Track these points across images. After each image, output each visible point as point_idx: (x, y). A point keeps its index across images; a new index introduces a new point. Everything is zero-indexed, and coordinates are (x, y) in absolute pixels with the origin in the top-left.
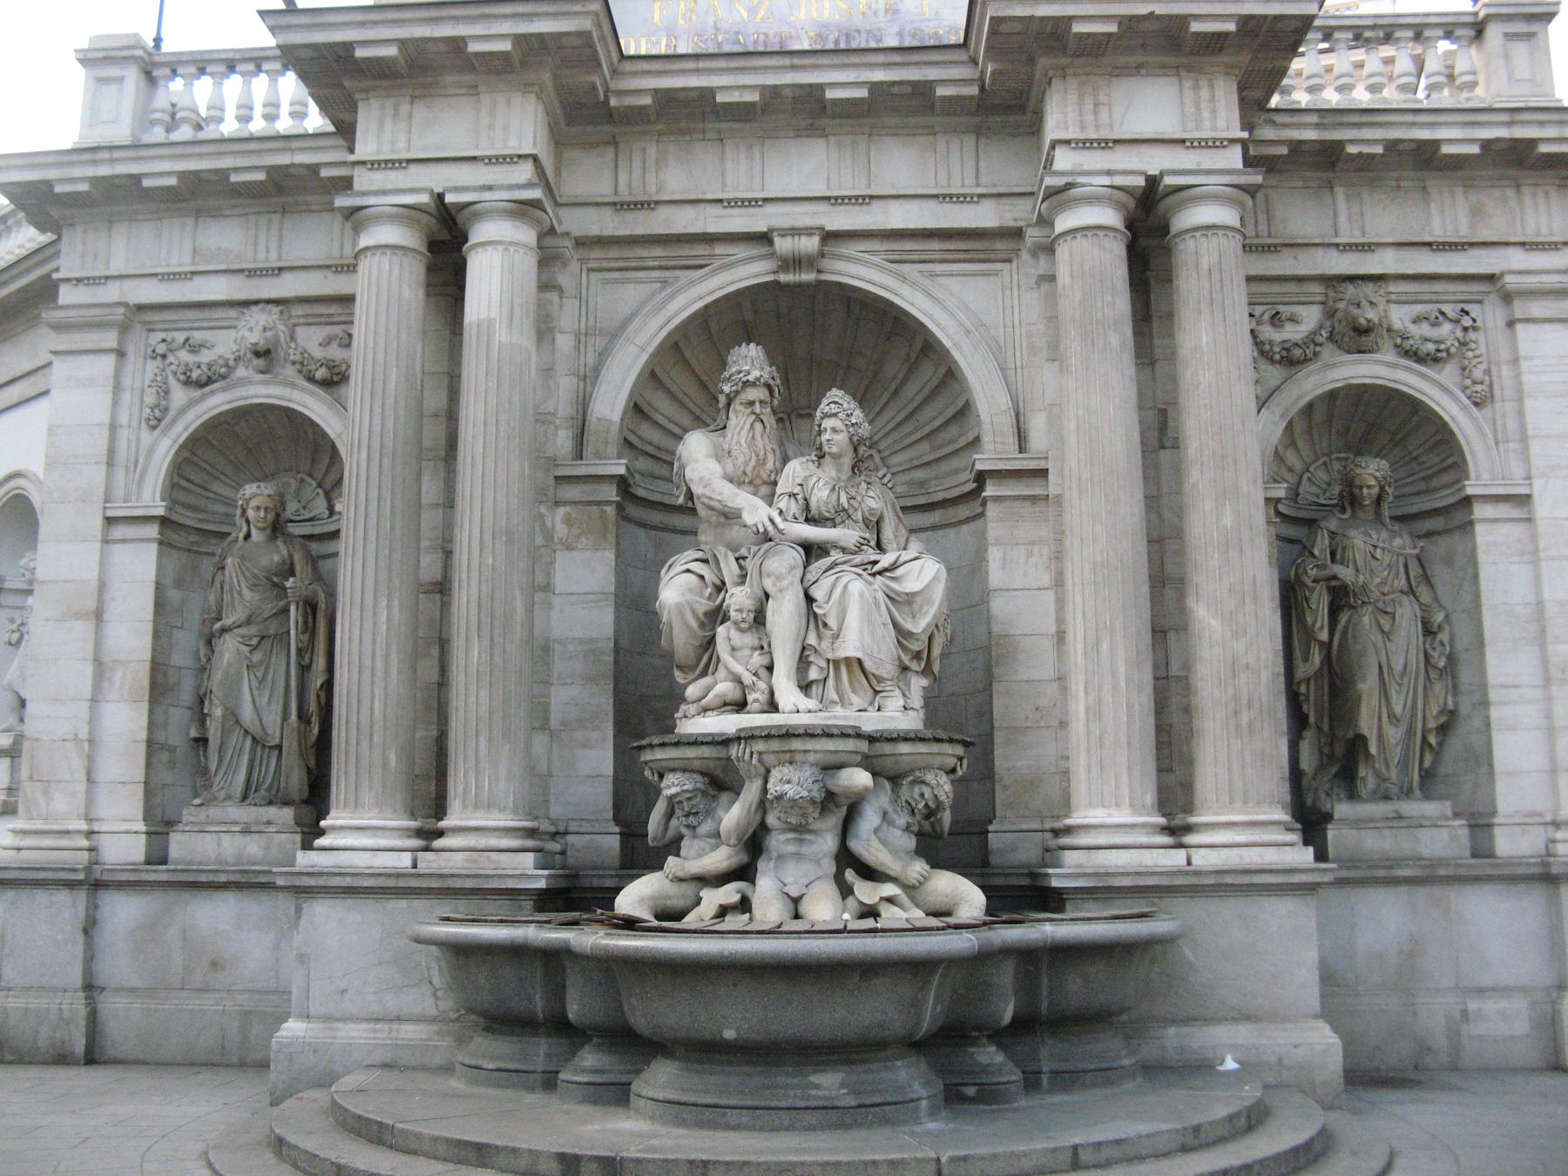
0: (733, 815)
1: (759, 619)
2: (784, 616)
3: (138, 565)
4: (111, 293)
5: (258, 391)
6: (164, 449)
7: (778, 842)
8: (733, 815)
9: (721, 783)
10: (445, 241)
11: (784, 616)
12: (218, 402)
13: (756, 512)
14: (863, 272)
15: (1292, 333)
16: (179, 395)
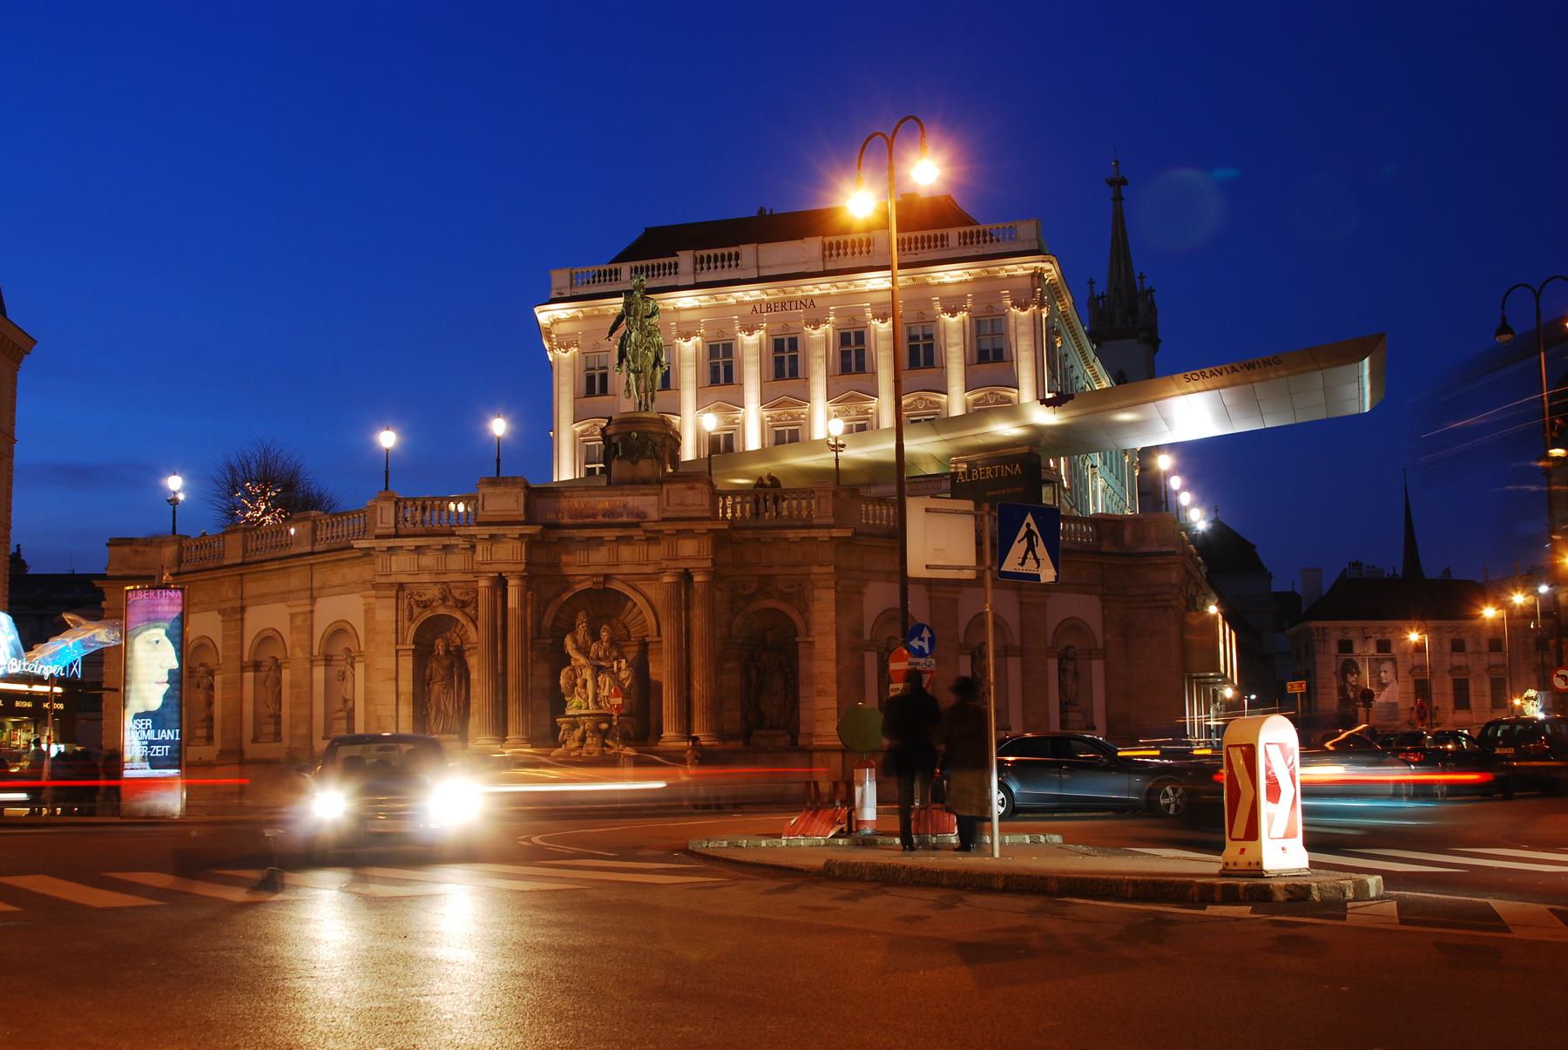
0: (578, 733)
1: (585, 686)
2: (590, 684)
3: (407, 664)
4: (392, 579)
5: (442, 611)
6: (413, 628)
7: (589, 741)
8: (578, 733)
9: (575, 726)
10: (500, 583)
11: (590, 684)
12: (428, 614)
13: (582, 661)
14: (616, 585)
15: (748, 592)
16: (416, 611)
